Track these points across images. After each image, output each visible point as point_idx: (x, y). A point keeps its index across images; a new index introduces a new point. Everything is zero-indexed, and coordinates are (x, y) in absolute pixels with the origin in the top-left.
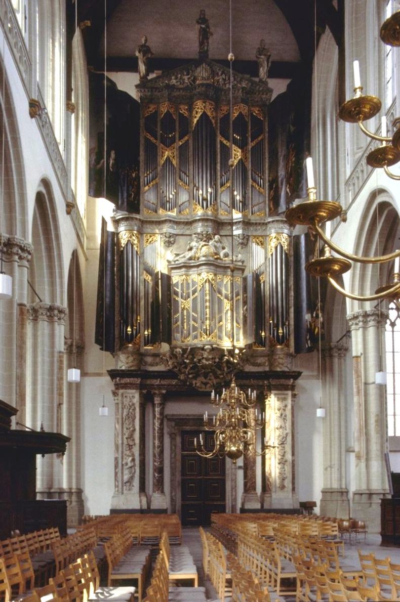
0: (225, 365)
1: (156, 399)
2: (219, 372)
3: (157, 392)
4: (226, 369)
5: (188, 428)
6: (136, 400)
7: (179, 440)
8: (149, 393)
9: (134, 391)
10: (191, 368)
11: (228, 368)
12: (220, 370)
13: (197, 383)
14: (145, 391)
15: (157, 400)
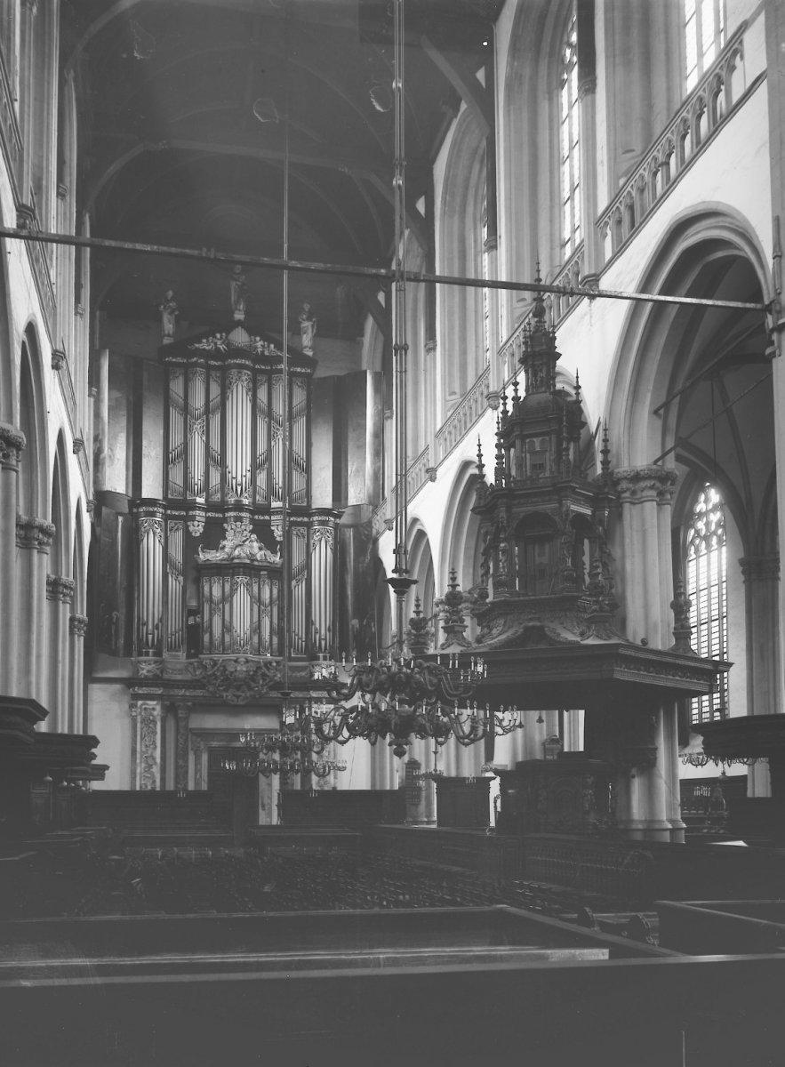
0: (260, 677)
1: (180, 712)
2: (253, 685)
3: (182, 704)
4: (261, 682)
5: (215, 744)
6: (158, 712)
7: (205, 757)
8: (173, 704)
9: (155, 702)
10: (223, 681)
11: (264, 680)
12: (254, 681)
13: (228, 695)
14: (167, 703)
15: (181, 714)
